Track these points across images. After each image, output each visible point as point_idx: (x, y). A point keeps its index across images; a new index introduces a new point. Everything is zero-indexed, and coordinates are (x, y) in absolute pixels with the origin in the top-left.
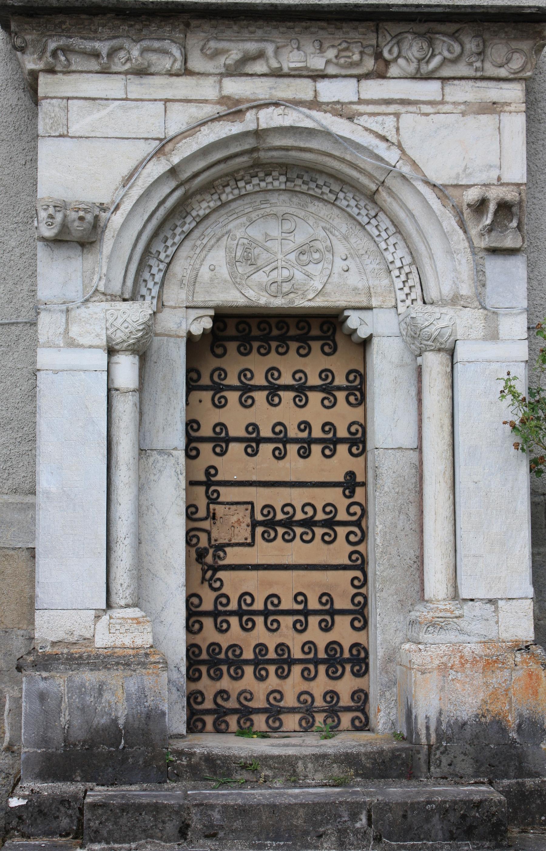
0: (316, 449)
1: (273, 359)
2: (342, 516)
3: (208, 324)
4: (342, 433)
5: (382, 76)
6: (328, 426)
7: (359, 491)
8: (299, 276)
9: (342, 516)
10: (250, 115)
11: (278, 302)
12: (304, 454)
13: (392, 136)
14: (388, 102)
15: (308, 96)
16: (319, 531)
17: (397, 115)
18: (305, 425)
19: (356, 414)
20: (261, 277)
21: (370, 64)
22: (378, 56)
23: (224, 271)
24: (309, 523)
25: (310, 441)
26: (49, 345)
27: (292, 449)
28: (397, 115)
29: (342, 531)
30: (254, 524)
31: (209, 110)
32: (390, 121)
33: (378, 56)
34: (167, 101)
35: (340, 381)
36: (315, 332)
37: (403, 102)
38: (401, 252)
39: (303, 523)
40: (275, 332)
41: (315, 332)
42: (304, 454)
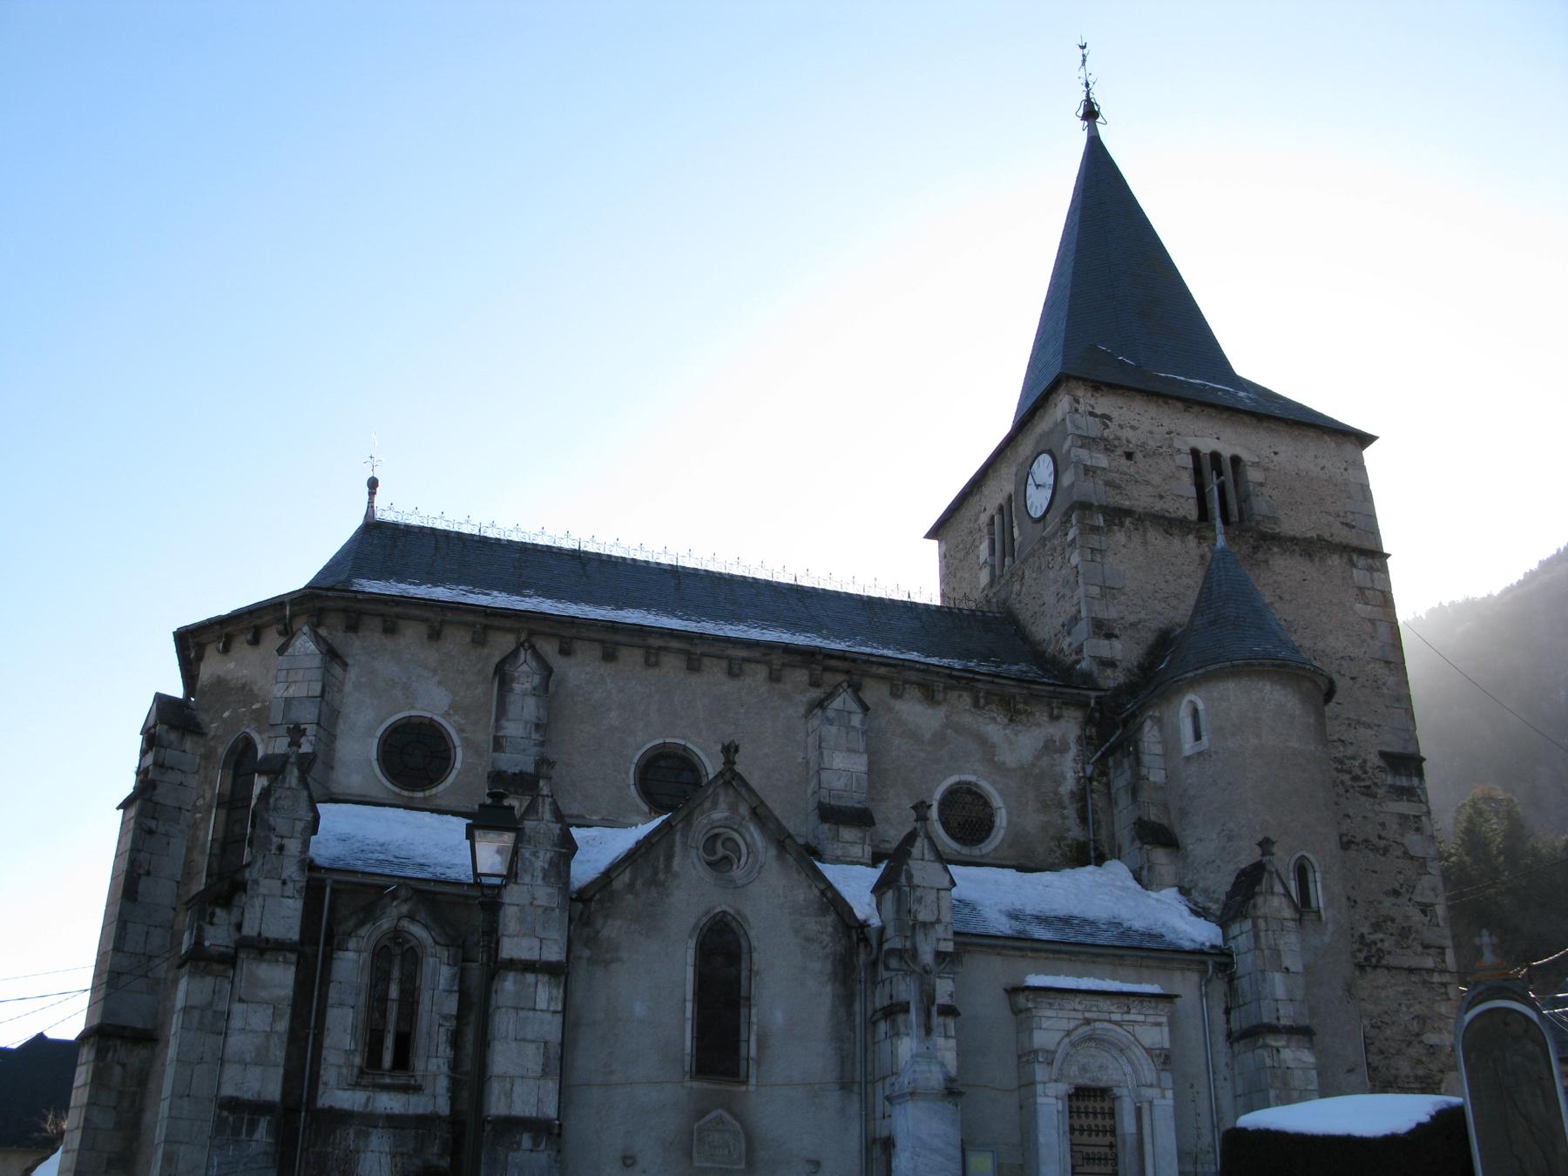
0: (1100, 1134)
1: (1087, 1103)
2: (1110, 1157)
3: (1073, 1090)
4: (1108, 1129)
5: (1128, 1013)
6: (1104, 1126)
7: (1114, 1149)
8: (1099, 1075)
9: (1110, 1157)
10: (1092, 1024)
11: (1094, 1084)
12: (1097, 1135)
13: (1131, 1031)
14: (1130, 1021)
15: (1108, 1018)
16: (1103, 1162)
17: (1133, 1026)
18: (1097, 1126)
19: (1112, 1122)
20: (1088, 1075)
21: (1126, 1009)
22: (1128, 1007)
23: (1077, 1073)
24: (1100, 1159)
25: (1098, 1131)
26: (1040, 1096)
27: (1093, 1134)
28: (1133, 1026)
29: (1110, 1162)
30: (1083, 1159)
31: (1081, 1022)
32: (1131, 1027)
33: (1128, 1007)
34: (1069, 1018)
35: (1107, 1111)
36: (1098, 1094)
37: (1135, 1022)
38: (1130, 1069)
39: (1098, 1159)
40: (1087, 1094)
41: (1098, 1094)
42: (1097, 1135)
